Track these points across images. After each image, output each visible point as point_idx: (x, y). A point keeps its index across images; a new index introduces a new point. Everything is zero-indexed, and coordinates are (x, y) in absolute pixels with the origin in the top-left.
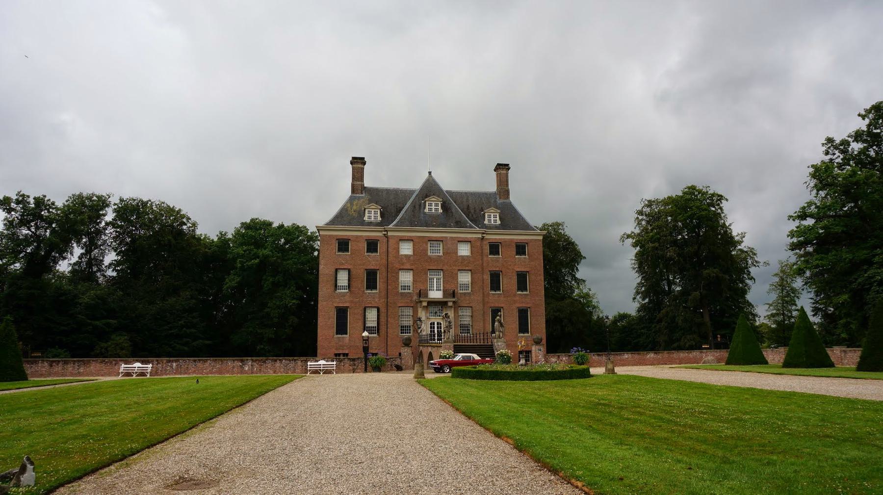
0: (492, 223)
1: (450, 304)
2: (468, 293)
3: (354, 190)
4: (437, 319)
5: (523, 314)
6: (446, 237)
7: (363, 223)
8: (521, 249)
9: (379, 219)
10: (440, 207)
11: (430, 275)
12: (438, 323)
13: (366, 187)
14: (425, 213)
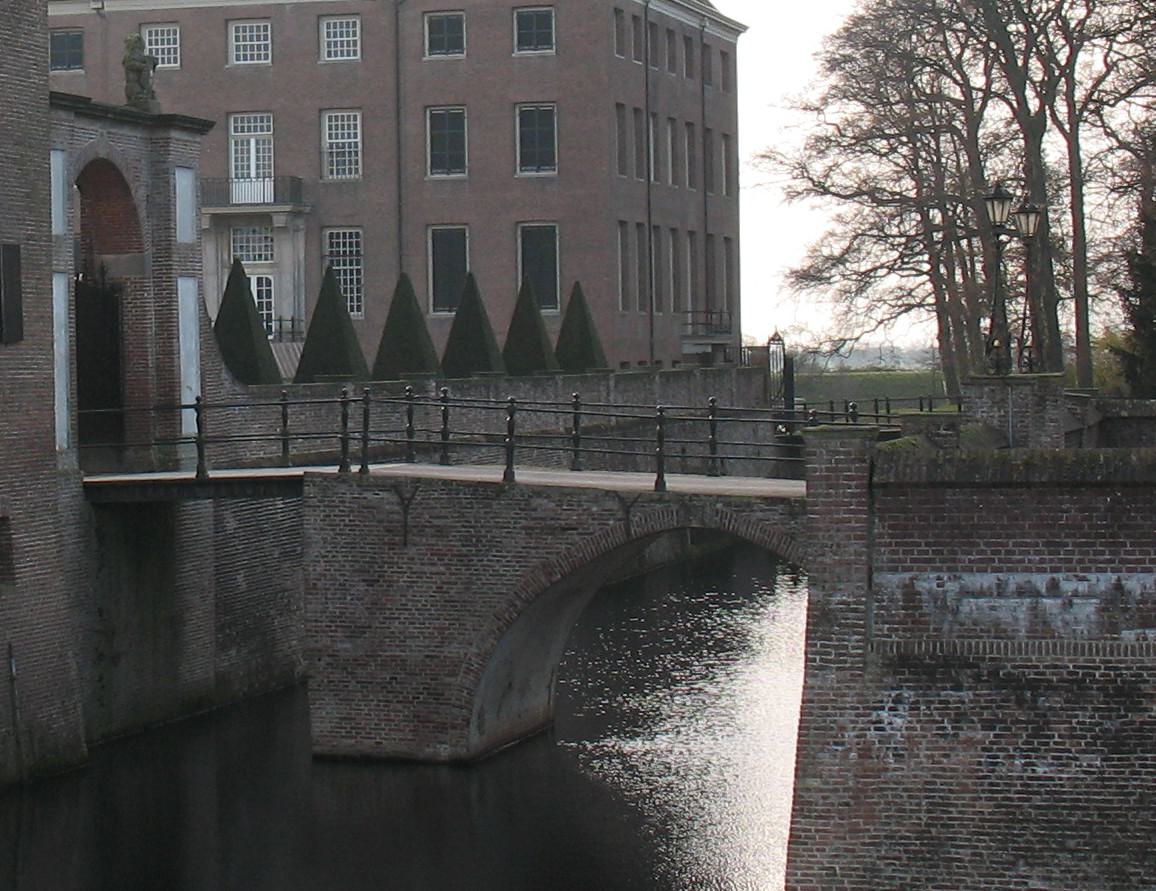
1: (279, 221)
12: (259, 280)
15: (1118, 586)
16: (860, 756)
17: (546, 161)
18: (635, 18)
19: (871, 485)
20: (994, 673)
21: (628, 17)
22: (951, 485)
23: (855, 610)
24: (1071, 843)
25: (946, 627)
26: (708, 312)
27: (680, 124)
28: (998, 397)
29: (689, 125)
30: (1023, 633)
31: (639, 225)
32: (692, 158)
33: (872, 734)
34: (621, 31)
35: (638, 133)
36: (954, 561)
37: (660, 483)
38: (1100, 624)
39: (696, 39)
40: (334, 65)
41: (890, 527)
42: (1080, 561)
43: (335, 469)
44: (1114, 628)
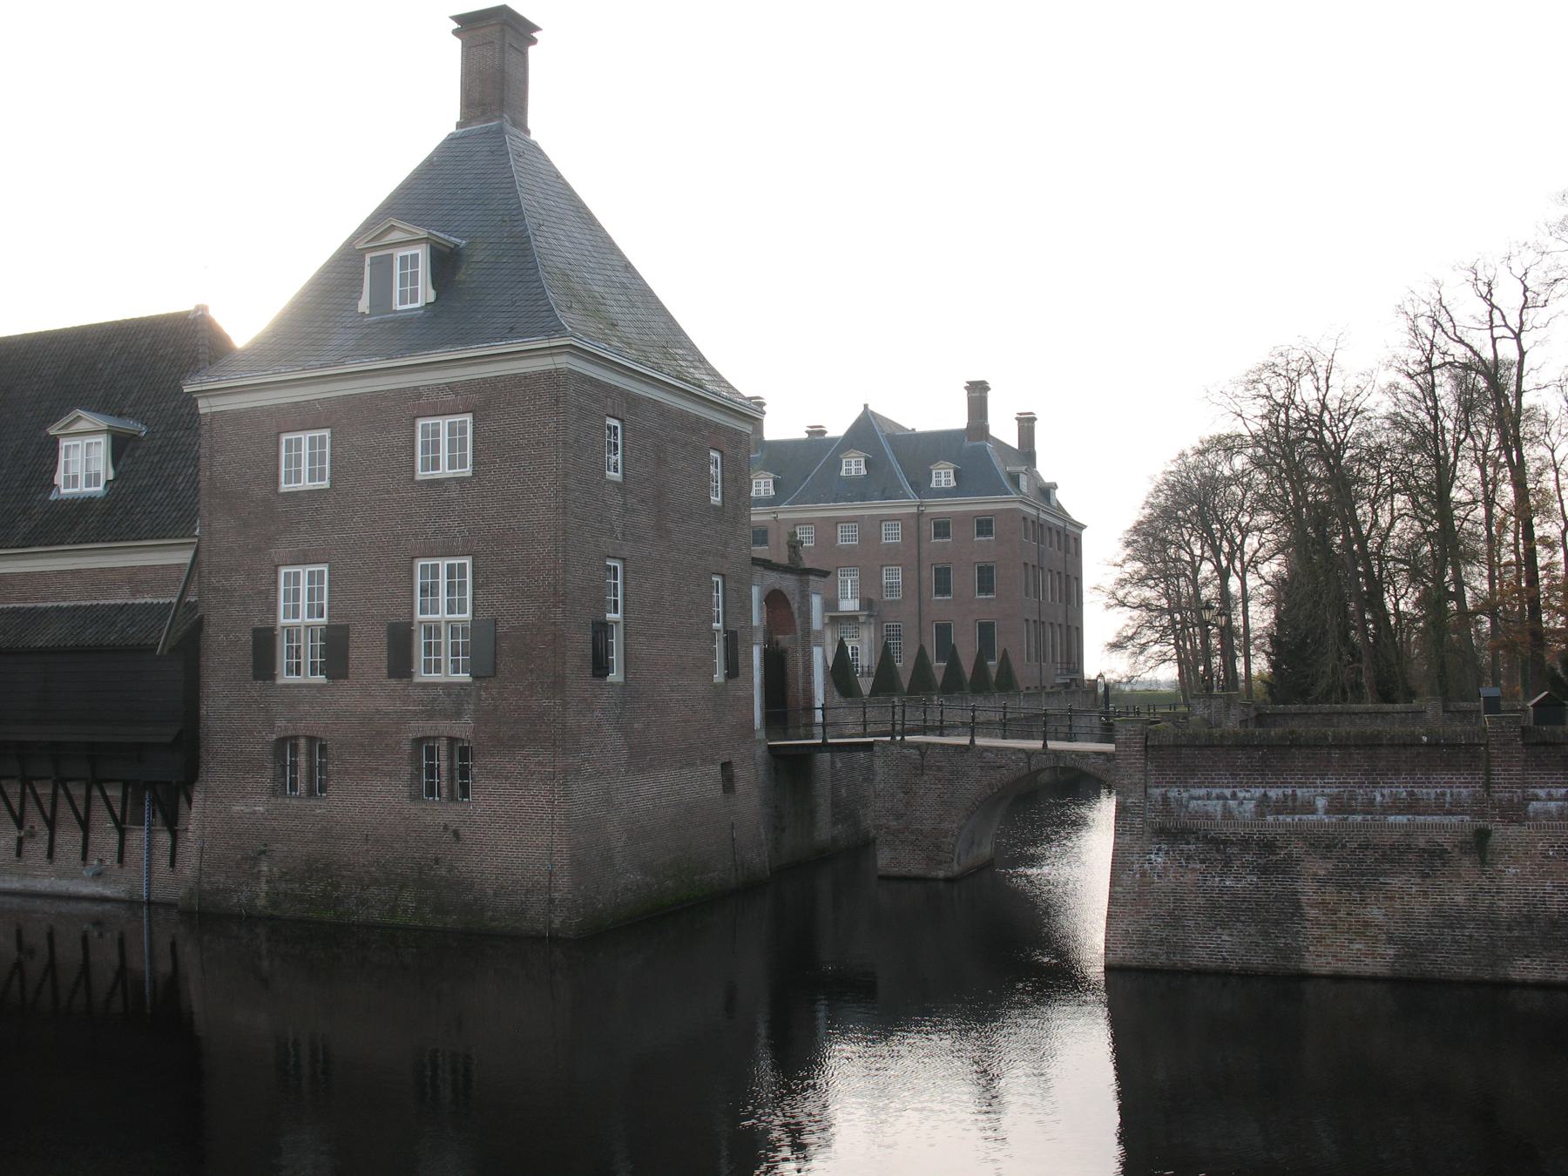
0: (943, 485)
1: (862, 619)
2: (899, 601)
9: (772, 493)
12: (852, 647)
13: (765, 441)
15: (1265, 795)
16: (1141, 876)
17: (990, 590)
18: (1033, 522)
19: (1146, 746)
20: (1205, 836)
21: (1030, 523)
22: (1185, 746)
23: (1139, 806)
24: (1242, 918)
25: (1182, 814)
26: (1068, 663)
27: (1055, 572)
28: (1208, 704)
29: (1059, 573)
30: (1219, 817)
31: (1035, 621)
32: (1060, 589)
33: (1146, 865)
34: (1026, 528)
35: (1035, 577)
36: (1186, 782)
37: (1045, 745)
38: (1256, 813)
39: (1062, 533)
40: (889, 544)
41: (1156, 766)
42: (1246, 783)
43: (889, 738)
44: (1263, 815)
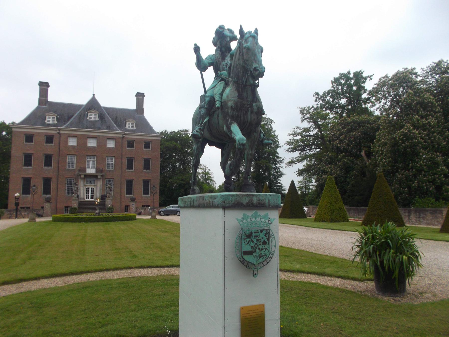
0: (131, 128)
1: (99, 177)
2: (113, 170)
3: (40, 102)
4: (92, 186)
5: (146, 183)
6: (99, 136)
7: (44, 124)
8: (147, 145)
9: (56, 122)
10: (97, 117)
11: (88, 159)
12: (91, 188)
14: (87, 120)
17: (148, 169)
